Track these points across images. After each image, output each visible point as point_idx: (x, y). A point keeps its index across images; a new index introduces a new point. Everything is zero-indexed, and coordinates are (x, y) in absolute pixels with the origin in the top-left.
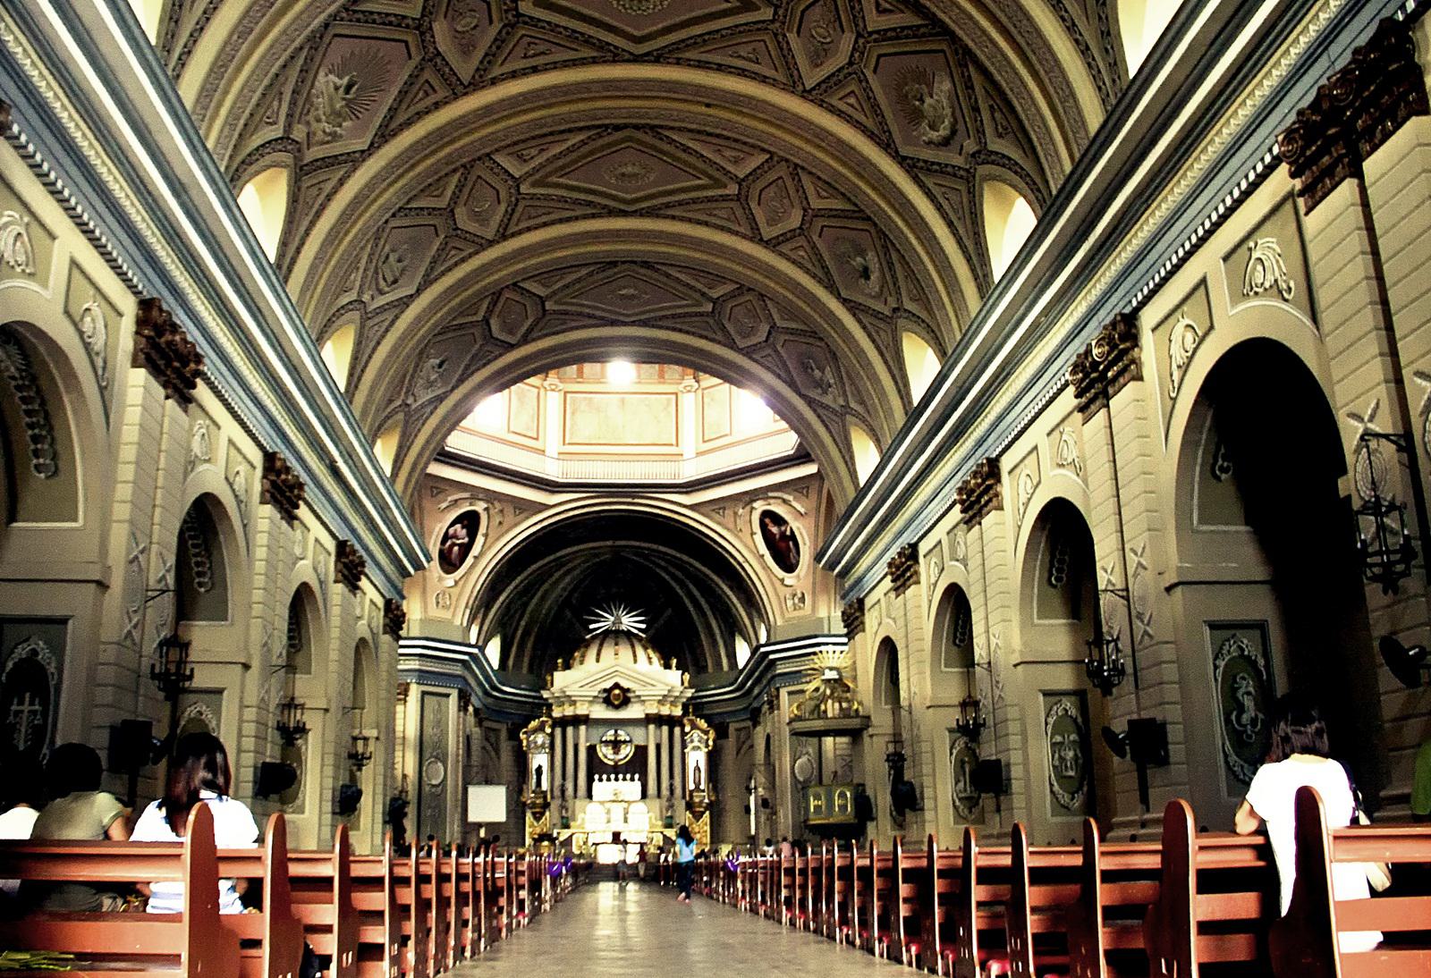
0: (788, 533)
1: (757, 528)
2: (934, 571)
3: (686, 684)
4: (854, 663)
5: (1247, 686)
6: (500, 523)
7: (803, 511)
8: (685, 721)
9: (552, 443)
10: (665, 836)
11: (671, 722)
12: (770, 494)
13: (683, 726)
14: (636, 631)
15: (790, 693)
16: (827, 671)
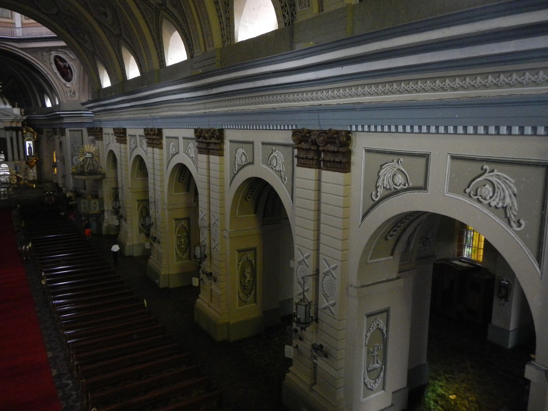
0: (67, 66)
1: (52, 61)
3: (23, 114)
5: (249, 270)
7: (73, 58)
10: (17, 177)
11: (17, 129)
12: (59, 50)
13: (22, 131)
15: (70, 131)
16: (87, 154)
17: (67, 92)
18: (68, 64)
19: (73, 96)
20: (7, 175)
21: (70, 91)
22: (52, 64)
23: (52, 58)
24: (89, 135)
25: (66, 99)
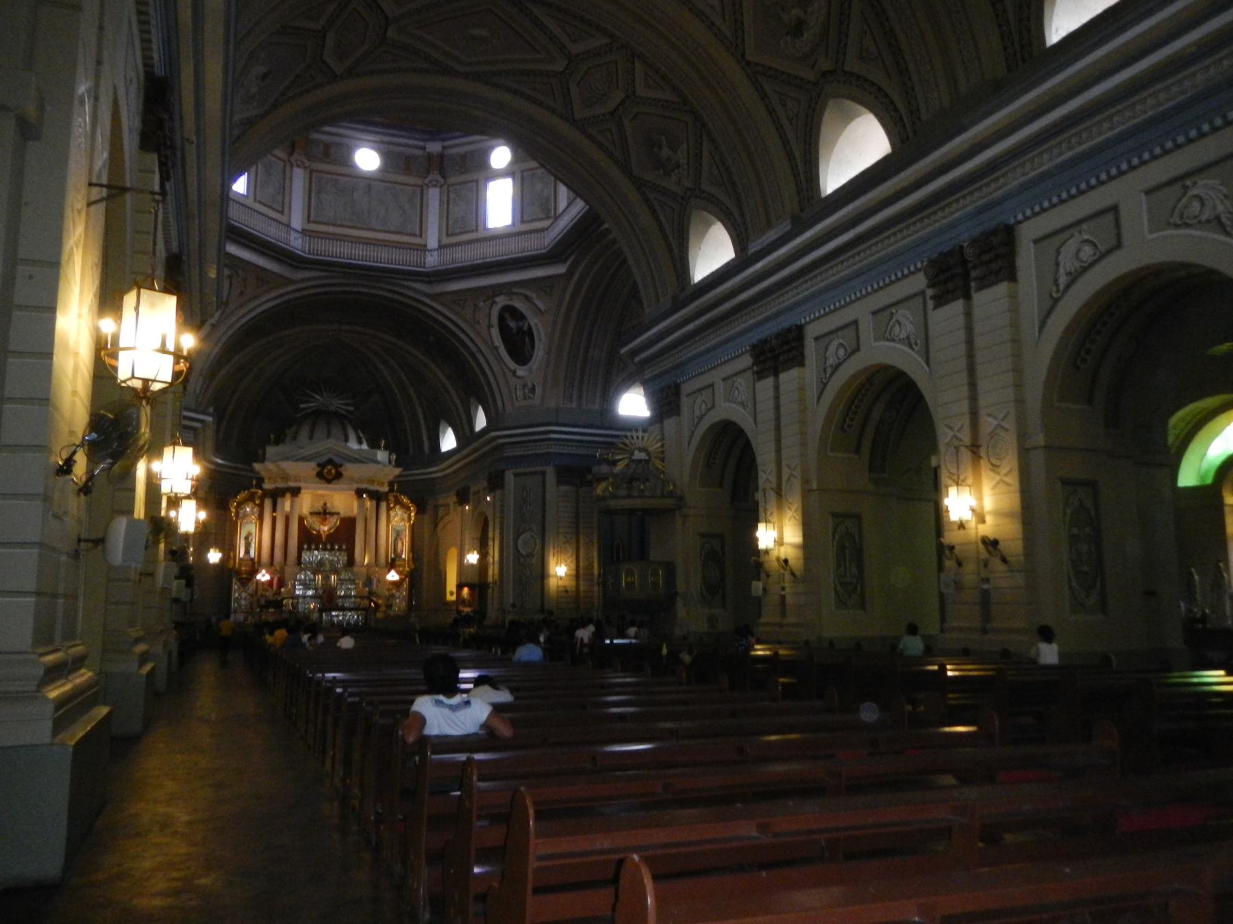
0: (526, 328)
1: (495, 320)
2: (834, 352)
4: (662, 446)
6: (242, 293)
8: (391, 497)
9: (297, 221)
12: (515, 290)
14: (342, 412)
15: (516, 475)
17: (516, 389)
18: (529, 325)
19: (530, 398)
20: (350, 596)
21: (524, 386)
22: (492, 326)
23: (495, 311)
24: (559, 483)
25: (513, 405)
